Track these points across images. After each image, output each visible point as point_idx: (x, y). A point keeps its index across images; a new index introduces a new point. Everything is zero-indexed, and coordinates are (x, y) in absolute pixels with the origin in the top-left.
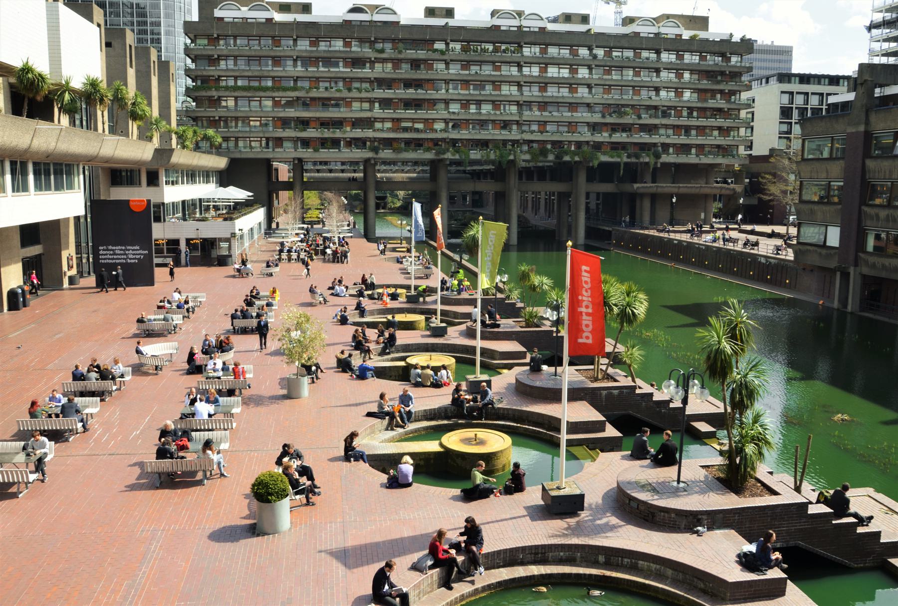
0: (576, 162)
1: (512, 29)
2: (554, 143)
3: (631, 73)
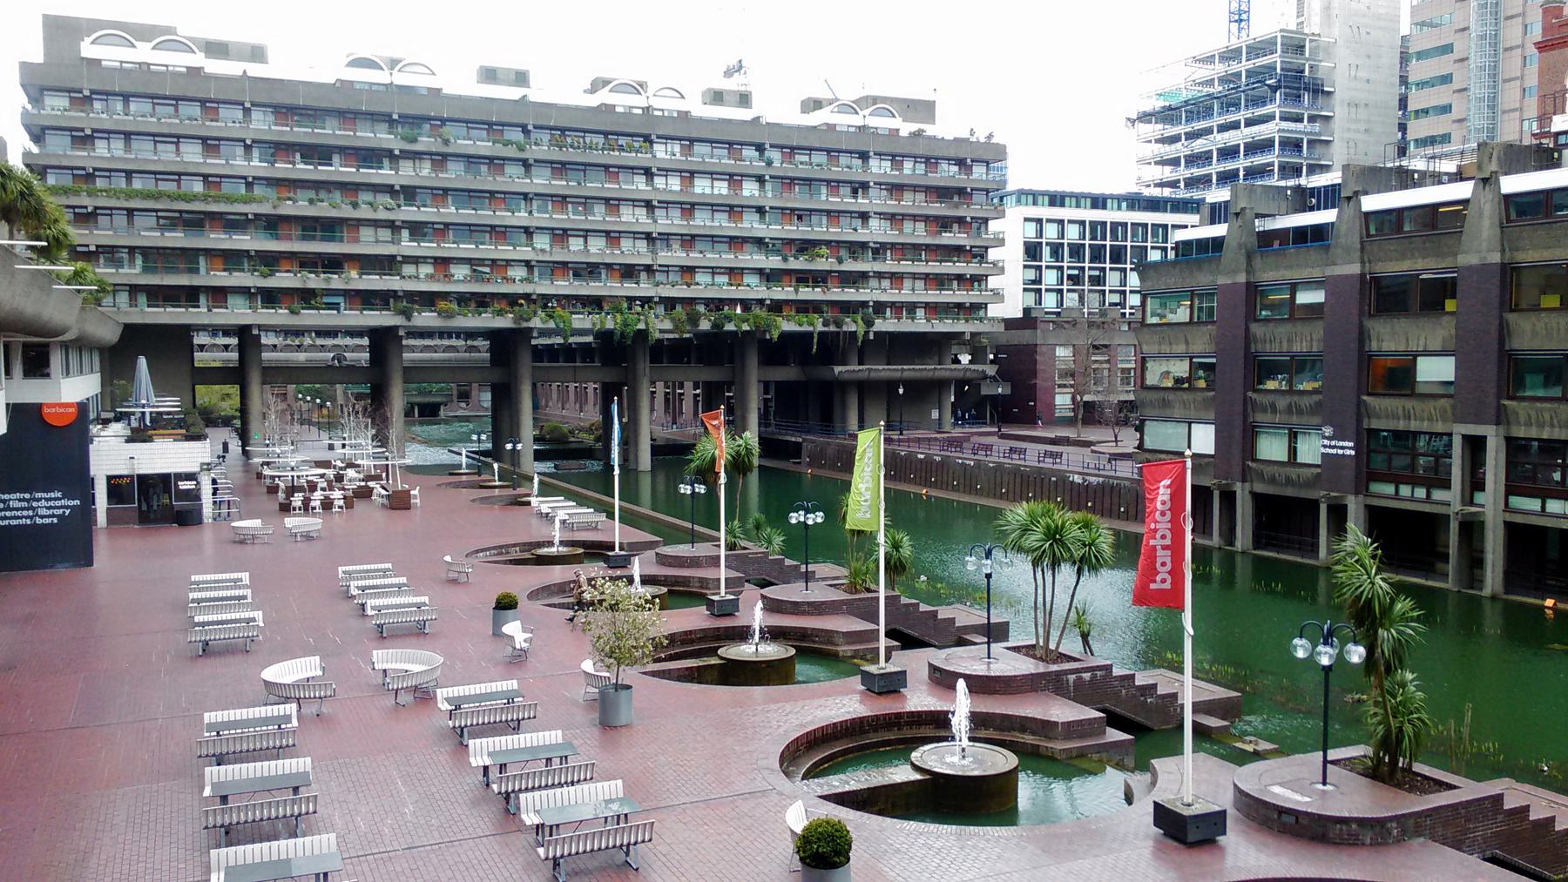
1: (635, 111)
2: (708, 302)
3: (824, 190)
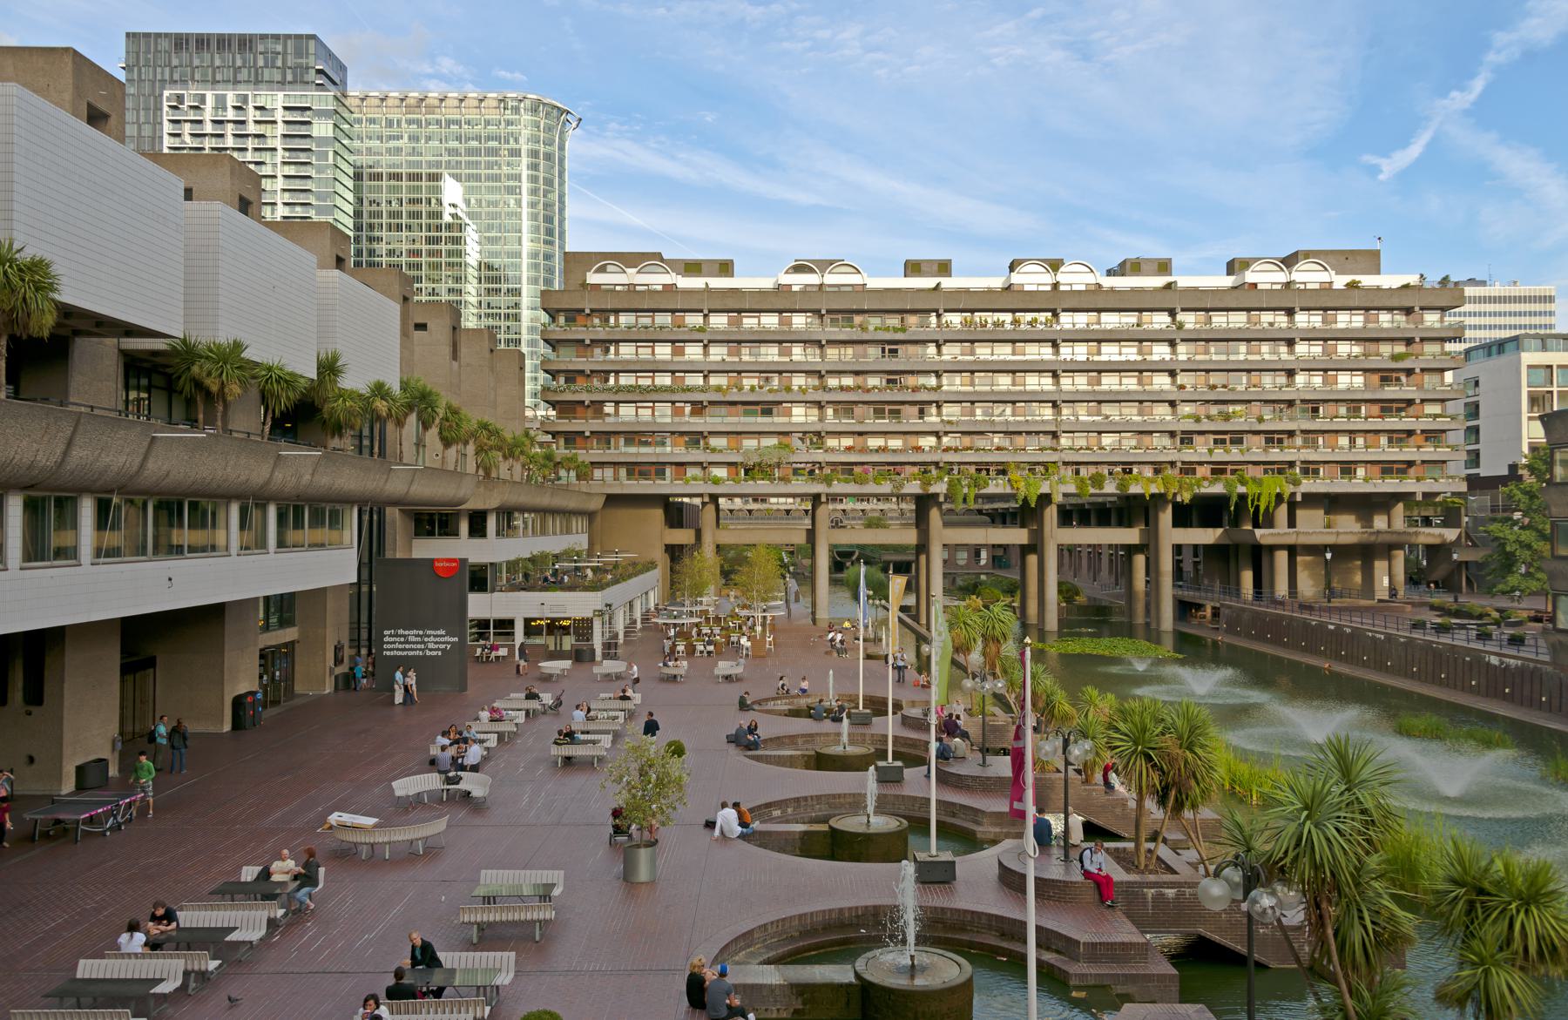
0: (1152, 496)
1: (1041, 288)
